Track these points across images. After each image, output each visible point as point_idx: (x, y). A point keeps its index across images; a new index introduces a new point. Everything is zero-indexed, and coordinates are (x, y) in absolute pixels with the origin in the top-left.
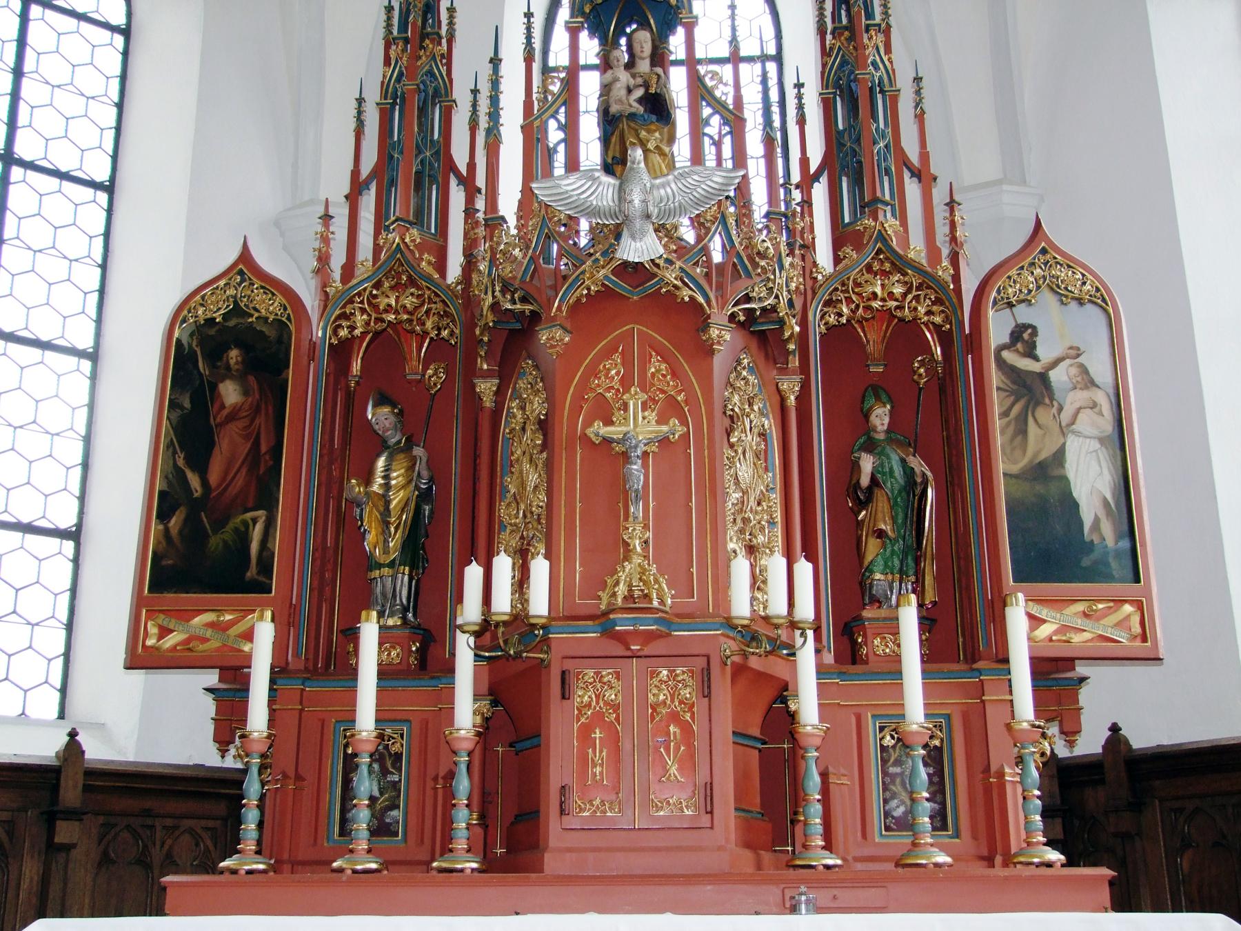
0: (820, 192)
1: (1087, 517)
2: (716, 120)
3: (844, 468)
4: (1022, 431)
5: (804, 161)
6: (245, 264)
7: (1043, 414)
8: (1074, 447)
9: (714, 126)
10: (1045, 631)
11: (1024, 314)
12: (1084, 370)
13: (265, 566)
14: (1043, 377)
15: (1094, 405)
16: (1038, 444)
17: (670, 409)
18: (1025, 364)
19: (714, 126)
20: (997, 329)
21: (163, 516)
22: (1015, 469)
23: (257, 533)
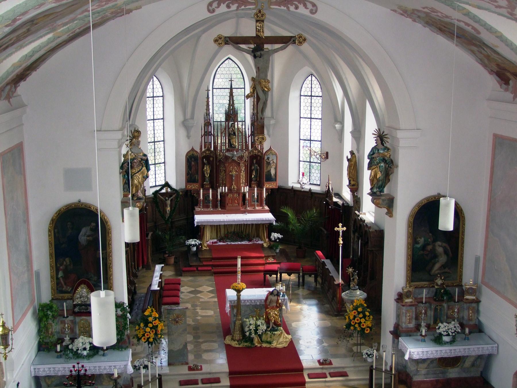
0: (250, 138)
1: (272, 175)
2: (240, 133)
3: (251, 167)
4: (267, 168)
5: (249, 134)
6: (193, 149)
7: (269, 166)
8: (272, 169)
9: (240, 135)
10: (268, 186)
11: (268, 156)
12: (273, 161)
13: (198, 181)
14: (270, 162)
15: (274, 165)
16: (268, 169)
17: (236, 171)
18: (268, 161)
19: (240, 135)
20: (266, 158)
21: (188, 175)
22: (266, 171)
23: (197, 177)
